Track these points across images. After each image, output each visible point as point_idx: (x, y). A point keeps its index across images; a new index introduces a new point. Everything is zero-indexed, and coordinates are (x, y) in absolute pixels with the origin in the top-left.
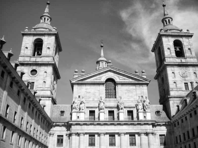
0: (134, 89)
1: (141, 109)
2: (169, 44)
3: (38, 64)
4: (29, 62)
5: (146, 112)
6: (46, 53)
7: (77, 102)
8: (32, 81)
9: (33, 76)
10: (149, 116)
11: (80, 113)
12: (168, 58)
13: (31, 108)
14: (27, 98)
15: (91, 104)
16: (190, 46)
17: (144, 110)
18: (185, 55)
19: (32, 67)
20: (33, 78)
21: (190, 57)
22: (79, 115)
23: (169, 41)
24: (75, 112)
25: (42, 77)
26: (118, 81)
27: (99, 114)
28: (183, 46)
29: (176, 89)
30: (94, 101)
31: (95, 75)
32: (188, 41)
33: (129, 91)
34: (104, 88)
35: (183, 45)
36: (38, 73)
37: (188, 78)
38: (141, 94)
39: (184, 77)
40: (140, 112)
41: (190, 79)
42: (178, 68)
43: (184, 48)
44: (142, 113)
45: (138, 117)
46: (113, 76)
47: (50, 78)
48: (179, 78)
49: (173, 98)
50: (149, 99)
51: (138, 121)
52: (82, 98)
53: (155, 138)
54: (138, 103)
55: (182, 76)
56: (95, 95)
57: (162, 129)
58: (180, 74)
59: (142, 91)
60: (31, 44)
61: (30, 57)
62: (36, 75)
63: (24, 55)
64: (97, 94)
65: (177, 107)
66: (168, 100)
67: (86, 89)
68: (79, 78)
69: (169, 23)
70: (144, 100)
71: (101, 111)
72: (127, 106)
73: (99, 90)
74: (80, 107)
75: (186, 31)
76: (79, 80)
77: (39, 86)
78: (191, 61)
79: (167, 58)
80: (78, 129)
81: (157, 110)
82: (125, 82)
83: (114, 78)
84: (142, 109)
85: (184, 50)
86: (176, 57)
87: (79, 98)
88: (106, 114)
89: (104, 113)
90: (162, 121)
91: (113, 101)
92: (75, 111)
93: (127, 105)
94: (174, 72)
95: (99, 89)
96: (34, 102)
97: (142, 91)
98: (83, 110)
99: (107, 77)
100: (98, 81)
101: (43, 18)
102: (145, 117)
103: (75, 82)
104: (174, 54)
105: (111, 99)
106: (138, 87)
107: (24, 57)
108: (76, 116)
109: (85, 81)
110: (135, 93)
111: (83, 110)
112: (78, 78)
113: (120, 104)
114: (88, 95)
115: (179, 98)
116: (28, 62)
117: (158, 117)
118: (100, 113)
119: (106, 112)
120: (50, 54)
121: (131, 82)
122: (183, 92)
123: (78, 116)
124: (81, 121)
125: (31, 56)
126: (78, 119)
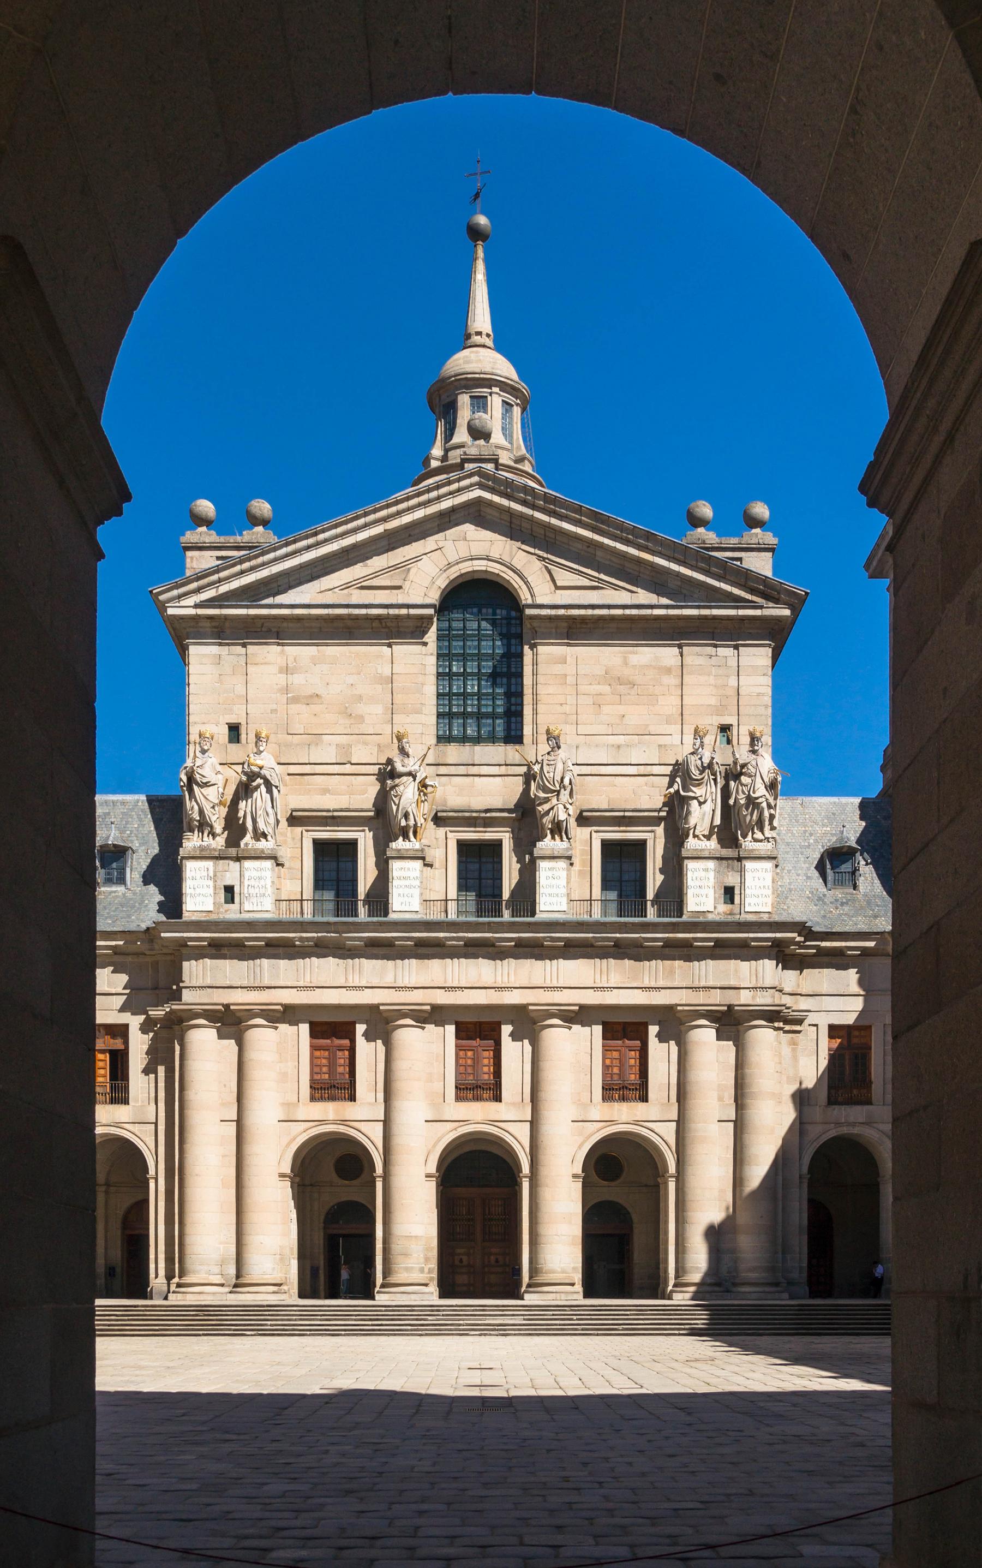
0: (668, 671)
1: (703, 829)
5: (739, 859)
7: (215, 774)
10: (761, 892)
11: (238, 859)
15: (325, 791)
22: (230, 873)
26: (539, 601)
30: (348, 769)
33: (622, 689)
34: (433, 659)
38: (720, 709)
45: (673, 893)
46: (506, 558)
50: (775, 758)
51: (674, 927)
52: (252, 746)
53: (794, 1050)
54: (685, 788)
56: (361, 719)
64: (374, 713)
67: (286, 670)
70: (735, 763)
71: (399, 844)
72: (604, 806)
74: (241, 814)
80: (228, 983)
83: (509, 576)
84: (712, 827)
87: (234, 746)
88: (438, 873)
89: (421, 862)
90: (863, 927)
91: (495, 770)
92: (202, 849)
93: (599, 795)
97: (733, 682)
98: (264, 835)
99: (450, 565)
102: (729, 893)
106: (698, 655)
108: (215, 887)
110: (670, 704)
111: (264, 835)
114: (302, 717)
117: (839, 893)
119: (436, 854)
123: (228, 883)
124: (250, 925)
126: (231, 905)
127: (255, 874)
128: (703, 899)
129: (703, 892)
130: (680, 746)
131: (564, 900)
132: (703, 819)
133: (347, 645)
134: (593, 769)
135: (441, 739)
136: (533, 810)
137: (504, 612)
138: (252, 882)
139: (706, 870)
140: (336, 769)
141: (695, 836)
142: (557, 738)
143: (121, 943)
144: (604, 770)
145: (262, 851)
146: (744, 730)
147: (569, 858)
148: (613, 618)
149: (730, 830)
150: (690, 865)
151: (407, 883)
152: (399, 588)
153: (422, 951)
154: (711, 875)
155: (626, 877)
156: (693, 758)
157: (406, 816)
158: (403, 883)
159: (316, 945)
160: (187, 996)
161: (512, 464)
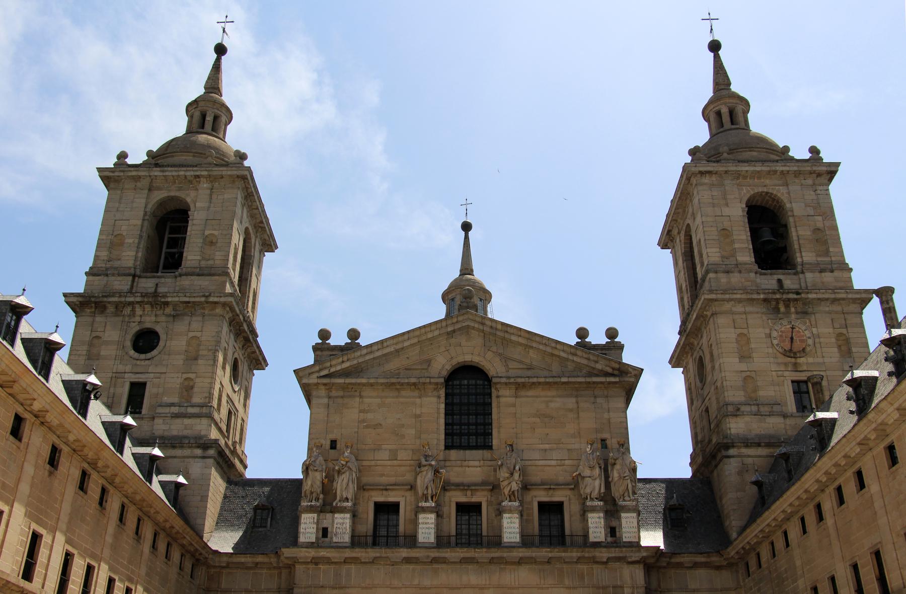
0: (571, 410)
1: (595, 494)
2: (726, 211)
3: (167, 304)
4: (126, 297)
6: (199, 258)
8: (138, 376)
9: (143, 356)
11: (331, 512)
12: (721, 275)
13: (89, 492)
14: (65, 449)
15: (383, 475)
16: (820, 218)
18: (799, 260)
19: (137, 319)
20: (143, 363)
21: (822, 266)
23: (725, 199)
24: (311, 509)
25: (181, 362)
28: (791, 219)
29: (754, 408)
31: (402, 348)
32: (815, 197)
34: (443, 406)
35: (790, 213)
36: (161, 343)
37: (811, 360)
39: (792, 352)
40: (594, 509)
41: (819, 363)
42: (764, 318)
43: (793, 229)
44: (602, 515)
47: (212, 362)
48: (772, 360)
49: (739, 447)
55: (780, 350)
56: (403, 436)
57: (693, 587)
58: (775, 342)
59: (606, 416)
60: (139, 222)
61: (134, 276)
62: (155, 352)
63: (107, 269)
65: (755, 488)
66: (719, 457)
68: (334, 362)
69: (732, 123)
73: (419, 416)
75: (807, 156)
76: (333, 370)
77: (166, 399)
78: (823, 283)
79: (716, 272)
82: (531, 380)
85: (795, 238)
86: (756, 267)
87: (333, 451)
88: (445, 520)
91: (477, 463)
92: (311, 506)
94: (745, 331)
95: (418, 412)
96: (107, 466)
97: (606, 416)
98: (347, 499)
101: (197, 114)
102: (612, 531)
103: (315, 381)
104: (747, 257)
105: (468, 452)
107: (107, 275)
108: (317, 529)
112: (328, 364)
115: (769, 445)
116: (123, 299)
120: (217, 262)
121: (558, 380)
122: (789, 421)
123: (325, 526)
125: (138, 272)
126: (326, 539)
127: (341, 521)
128: (599, 534)
129: (598, 530)
131: (518, 536)
132: (594, 489)
133: (397, 397)
135: (447, 447)
137: (481, 382)
138: (339, 526)
139: (599, 518)
140: (389, 463)
141: (592, 499)
142: (511, 445)
144: (538, 463)
145: (345, 508)
146: (614, 441)
148: (539, 383)
150: (590, 515)
151: (428, 526)
153: (435, 566)
154: (602, 521)
155: (552, 523)
157: (427, 488)
158: (425, 526)
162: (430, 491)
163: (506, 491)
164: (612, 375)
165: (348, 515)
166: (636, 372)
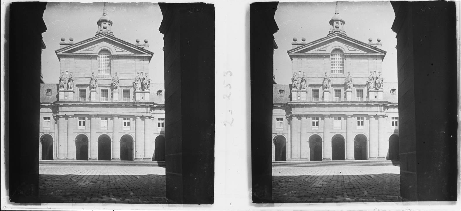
0: (133, 64)
5: (144, 93)
17: (143, 90)
26: (114, 53)
27: (90, 93)
30: (85, 78)
59: (143, 66)
81: (159, 90)
84: (140, 88)
98: (72, 88)
100: (89, 53)
103: (61, 54)
109: (74, 52)
111: (72, 88)
113: (114, 82)
118: (92, 93)
130: (135, 75)
134: (123, 79)
136: (113, 85)
143: (50, 104)
147: (118, 92)
149: (143, 87)
152: (92, 51)
156: (137, 77)
159: (313, 105)
160: (60, 113)
161: (110, 33)
162: (94, 86)
163: (115, 87)
164: (145, 54)
165: (72, 92)
166: (152, 54)
